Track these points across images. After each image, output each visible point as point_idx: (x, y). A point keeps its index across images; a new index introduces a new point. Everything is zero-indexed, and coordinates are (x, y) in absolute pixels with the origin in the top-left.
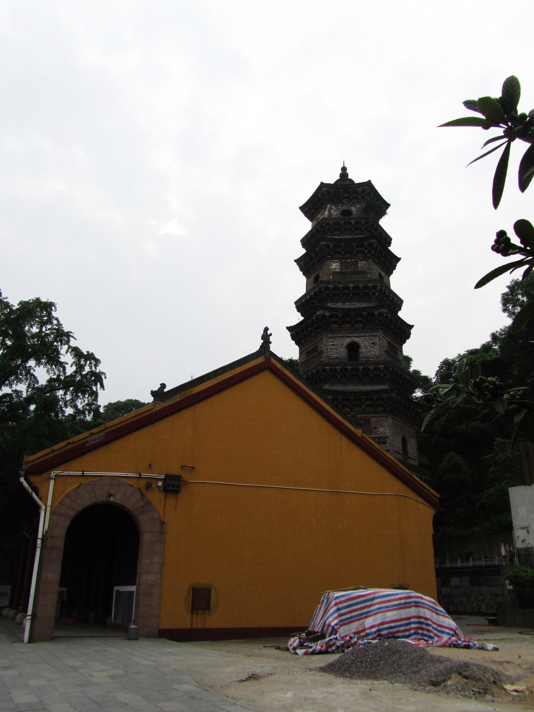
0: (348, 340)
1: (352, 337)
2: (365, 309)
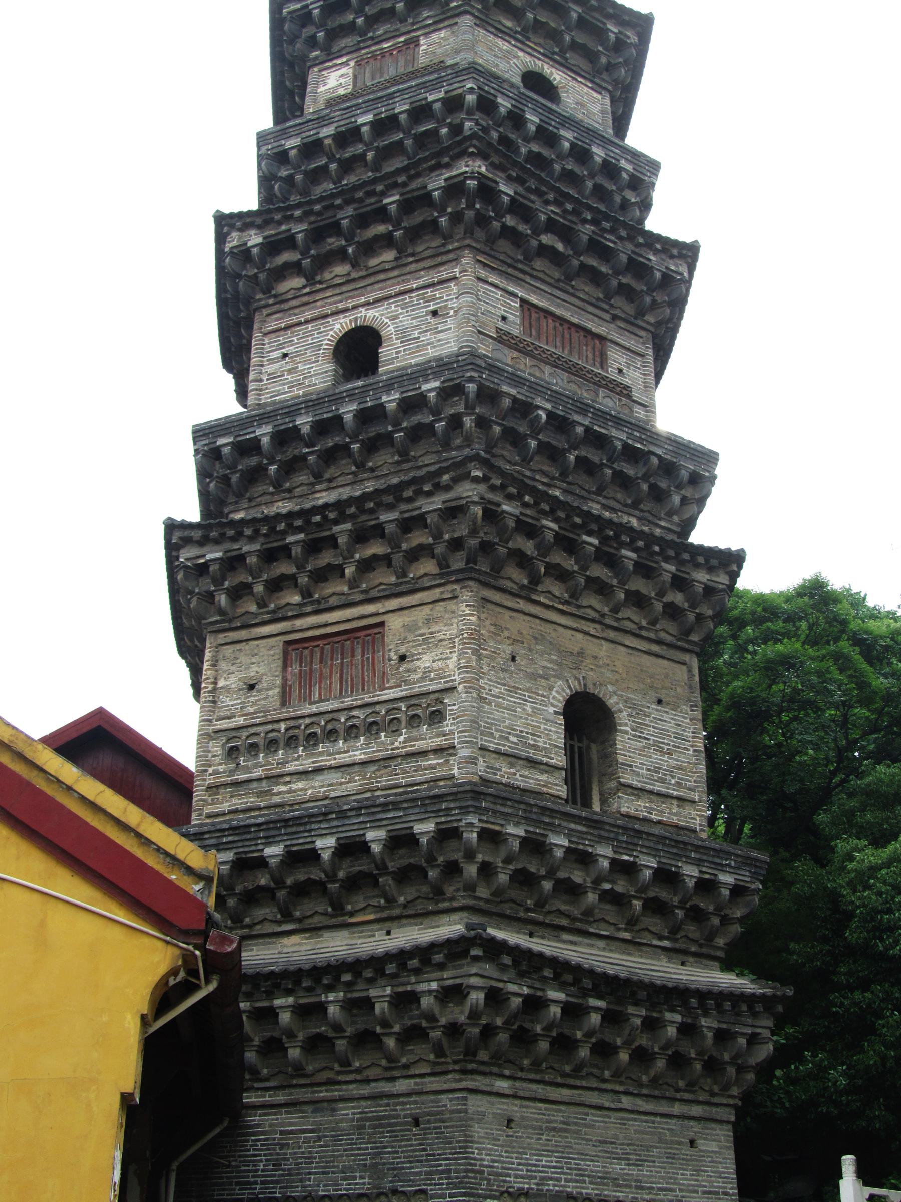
0: (340, 325)
1: (355, 307)
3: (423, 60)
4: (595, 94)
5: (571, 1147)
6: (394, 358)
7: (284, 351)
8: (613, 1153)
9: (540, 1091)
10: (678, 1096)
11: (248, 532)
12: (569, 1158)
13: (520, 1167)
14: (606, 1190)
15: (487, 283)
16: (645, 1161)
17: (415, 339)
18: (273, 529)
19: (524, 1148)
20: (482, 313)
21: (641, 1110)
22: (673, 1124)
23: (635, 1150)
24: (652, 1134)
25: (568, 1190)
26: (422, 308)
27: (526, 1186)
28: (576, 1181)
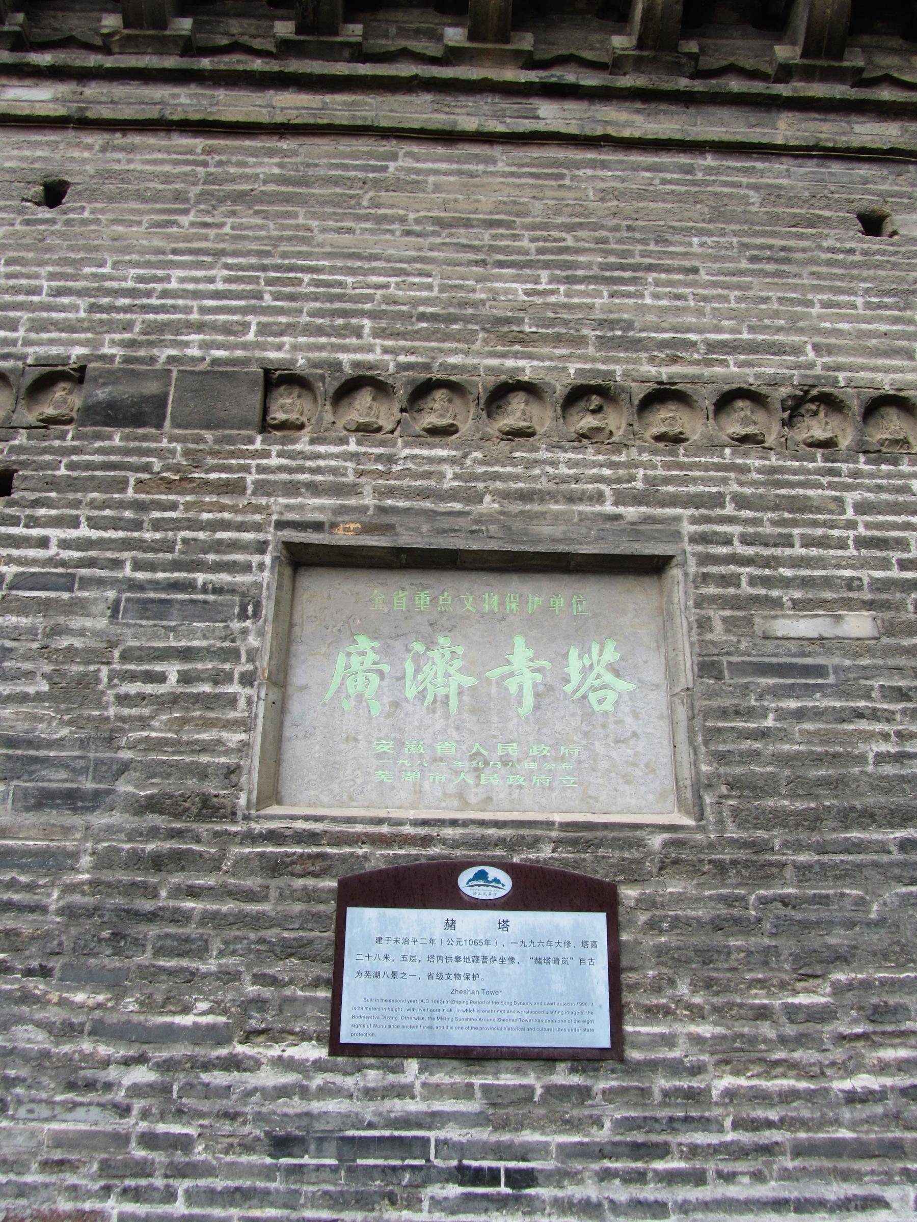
5: (305, 241)
8: (492, 249)
9: (184, 100)
10: (784, 90)
12: (291, 269)
13: (65, 300)
14: (456, 352)
16: (650, 268)
19: (97, 249)
21: (626, 133)
22: (777, 172)
23: (604, 241)
24: (679, 198)
25: (273, 355)
27: (78, 351)
28: (320, 331)
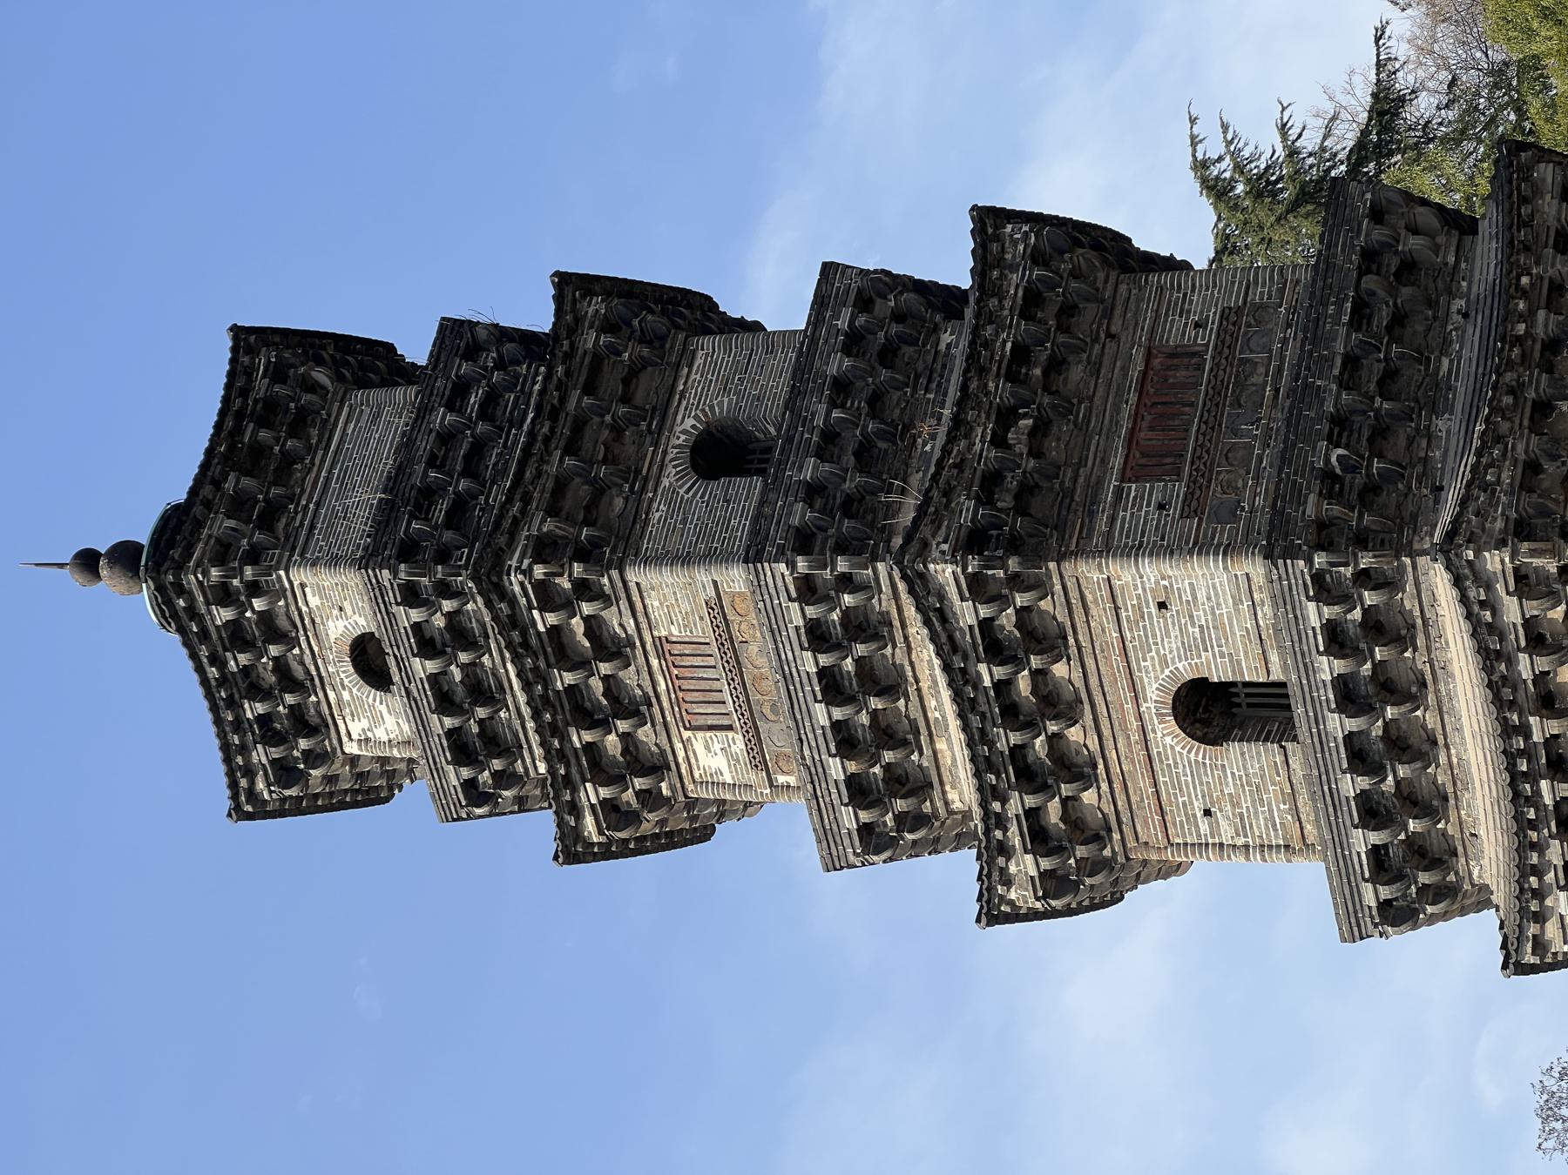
0: (1168, 736)
1: (1140, 717)
2: (960, 680)
3: (702, 630)
4: (699, 361)
6: (1231, 661)
7: (1199, 814)
11: (1534, 858)
15: (1110, 533)
17: (1202, 632)
18: (1532, 824)
20: (1163, 539)
26: (1152, 624)
